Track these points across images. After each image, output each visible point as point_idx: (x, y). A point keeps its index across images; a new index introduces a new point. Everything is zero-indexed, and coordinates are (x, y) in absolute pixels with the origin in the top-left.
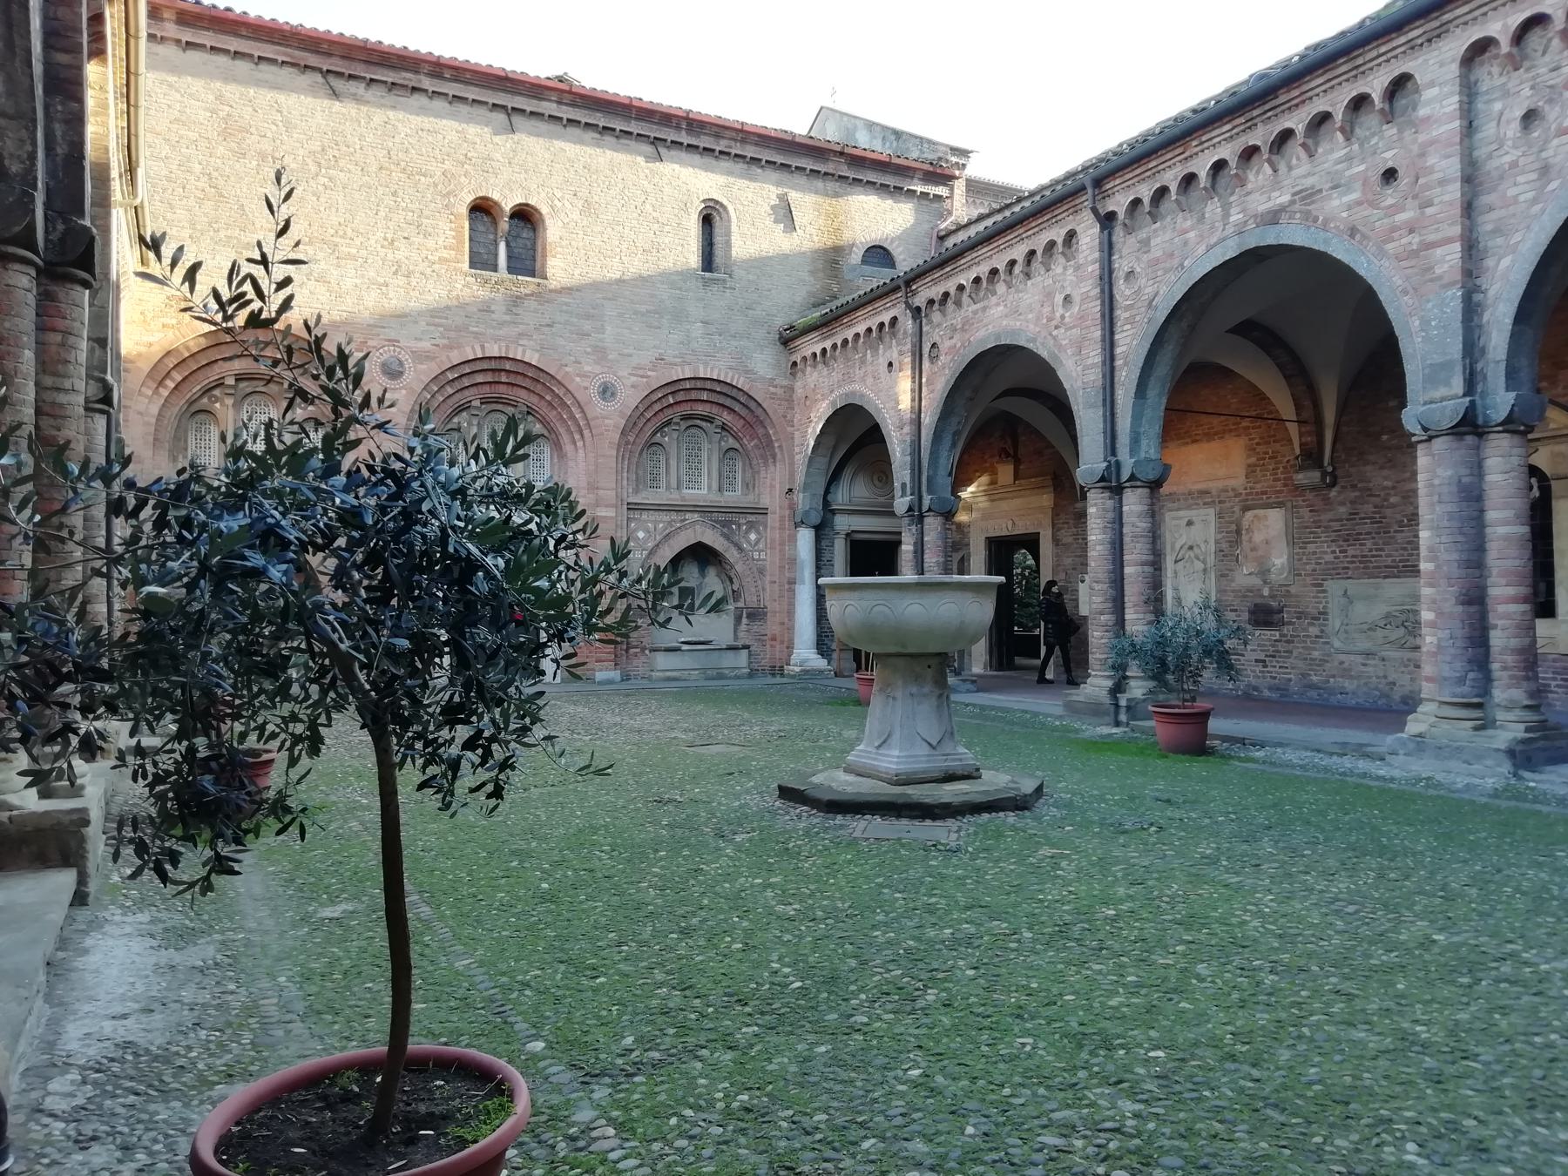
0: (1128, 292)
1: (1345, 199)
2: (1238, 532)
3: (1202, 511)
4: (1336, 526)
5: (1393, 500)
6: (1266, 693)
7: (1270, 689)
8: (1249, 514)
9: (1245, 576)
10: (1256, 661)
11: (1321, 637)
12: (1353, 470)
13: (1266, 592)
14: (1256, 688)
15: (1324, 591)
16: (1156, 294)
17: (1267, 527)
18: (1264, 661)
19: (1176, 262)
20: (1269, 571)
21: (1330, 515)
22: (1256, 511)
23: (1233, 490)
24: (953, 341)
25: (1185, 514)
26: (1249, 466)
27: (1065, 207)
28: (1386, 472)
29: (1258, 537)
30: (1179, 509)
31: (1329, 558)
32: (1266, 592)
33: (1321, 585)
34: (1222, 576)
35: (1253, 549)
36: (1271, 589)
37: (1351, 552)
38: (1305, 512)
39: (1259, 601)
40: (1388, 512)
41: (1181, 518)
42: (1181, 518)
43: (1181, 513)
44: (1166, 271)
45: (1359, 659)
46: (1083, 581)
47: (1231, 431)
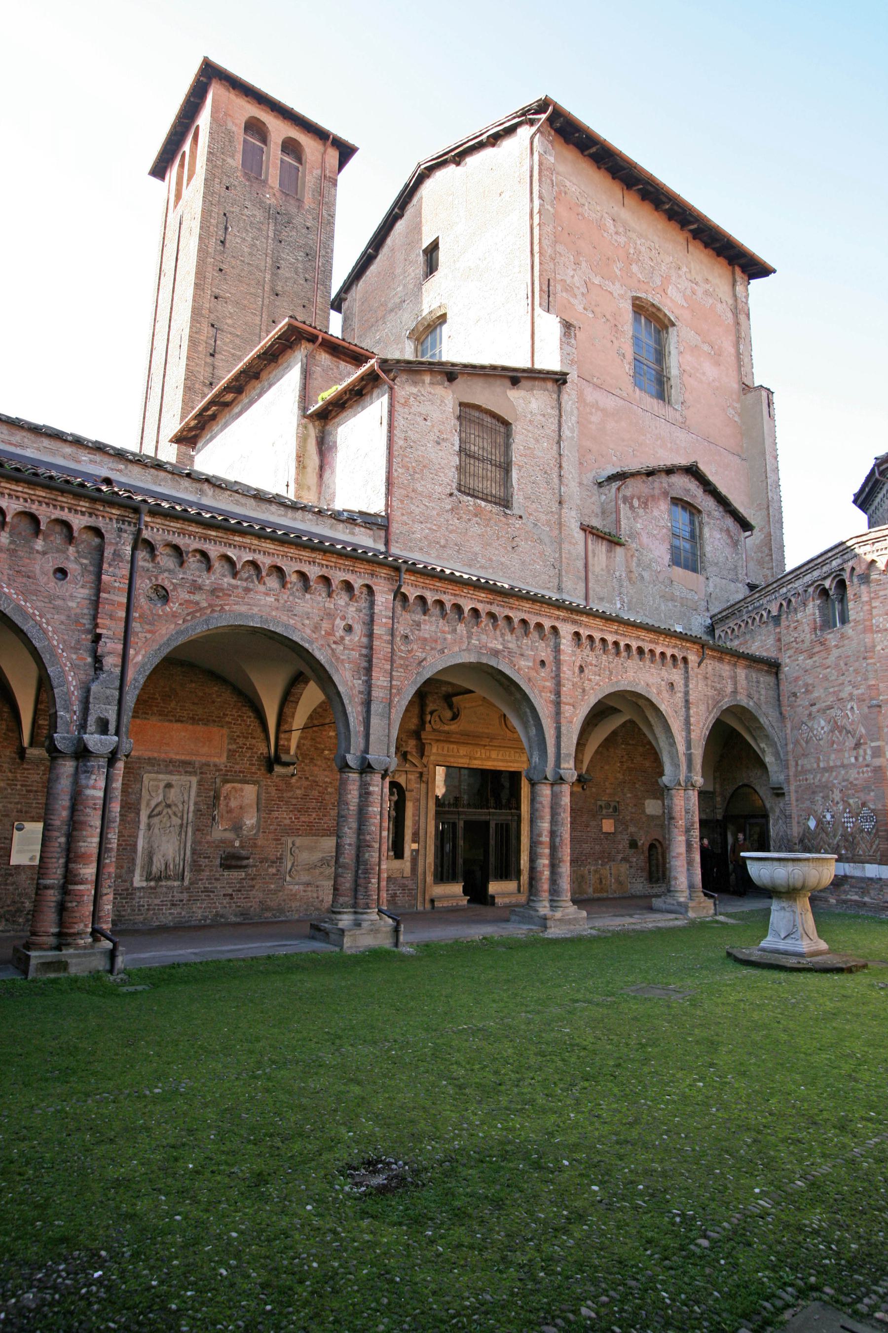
0: (402, 647)
1: (527, 664)
2: (216, 797)
3: (185, 778)
4: (294, 801)
5: (329, 790)
6: (233, 919)
7: (236, 915)
8: (228, 786)
9: (220, 832)
10: (224, 895)
11: (277, 875)
12: (306, 768)
13: (237, 844)
14: (222, 916)
15: (282, 844)
16: (425, 659)
17: (242, 796)
18: (232, 895)
19: (439, 647)
20: (241, 828)
21: (290, 794)
22: (236, 785)
23: (215, 765)
24: (196, 597)
25: (164, 778)
26: (230, 750)
27: (366, 567)
28: (326, 773)
29: (233, 804)
30: (158, 773)
31: (287, 822)
32: (237, 844)
33: (280, 840)
34: (198, 830)
35: (230, 811)
36: (241, 842)
37: (303, 819)
38: (272, 790)
39: (229, 850)
40: (327, 797)
41: (160, 780)
42: (160, 780)
43: (161, 776)
44: (432, 649)
45: (302, 888)
46: (20, 829)
47: (214, 721)
